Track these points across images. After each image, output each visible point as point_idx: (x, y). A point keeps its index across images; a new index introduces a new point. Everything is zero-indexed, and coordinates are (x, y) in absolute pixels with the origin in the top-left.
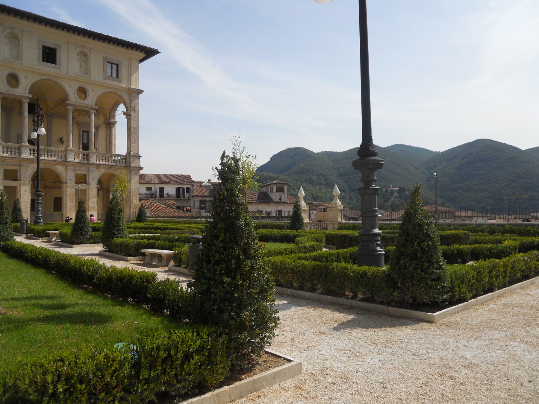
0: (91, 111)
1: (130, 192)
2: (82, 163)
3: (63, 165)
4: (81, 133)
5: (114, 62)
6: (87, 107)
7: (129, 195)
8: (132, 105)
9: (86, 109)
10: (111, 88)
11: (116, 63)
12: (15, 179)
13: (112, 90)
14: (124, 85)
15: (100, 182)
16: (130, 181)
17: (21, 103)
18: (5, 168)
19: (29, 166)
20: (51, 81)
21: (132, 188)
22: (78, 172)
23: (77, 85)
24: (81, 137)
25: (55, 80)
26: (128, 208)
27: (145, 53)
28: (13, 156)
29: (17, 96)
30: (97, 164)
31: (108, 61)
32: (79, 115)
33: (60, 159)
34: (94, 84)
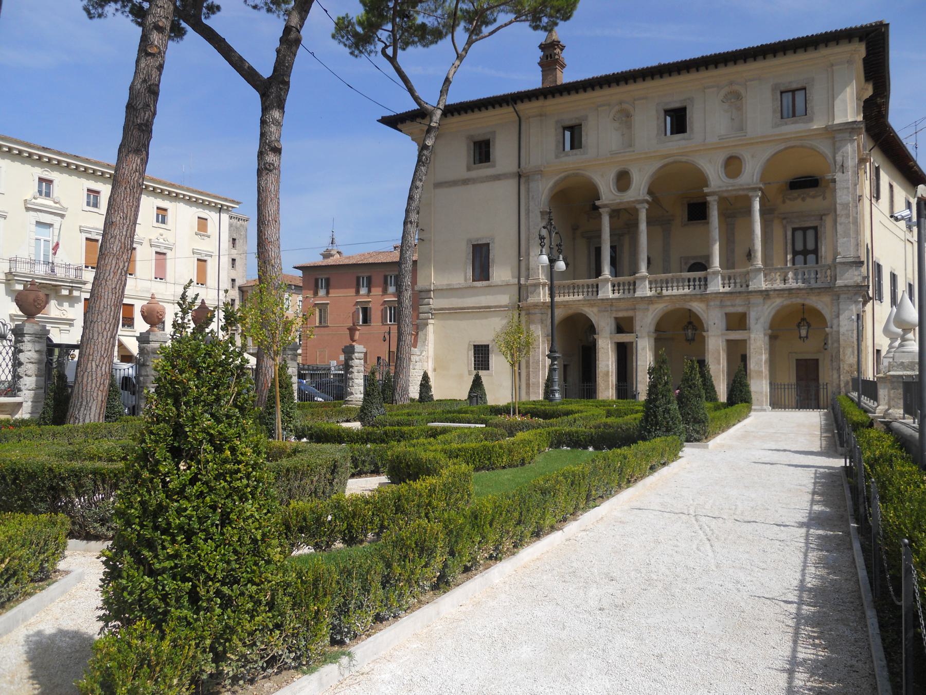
0: (751, 194)
4: (789, 234)
5: (794, 86)
6: (743, 190)
7: (836, 345)
8: (839, 158)
9: (741, 193)
10: (789, 139)
11: (799, 86)
12: (631, 331)
16: (838, 316)
18: (614, 315)
19: (647, 309)
21: (842, 330)
23: (721, 157)
25: (684, 159)
26: (835, 372)
27: (861, 40)
28: (627, 295)
29: (628, 202)
30: (761, 291)
31: (783, 89)
32: (784, 202)
33: (697, 291)
34: (752, 144)
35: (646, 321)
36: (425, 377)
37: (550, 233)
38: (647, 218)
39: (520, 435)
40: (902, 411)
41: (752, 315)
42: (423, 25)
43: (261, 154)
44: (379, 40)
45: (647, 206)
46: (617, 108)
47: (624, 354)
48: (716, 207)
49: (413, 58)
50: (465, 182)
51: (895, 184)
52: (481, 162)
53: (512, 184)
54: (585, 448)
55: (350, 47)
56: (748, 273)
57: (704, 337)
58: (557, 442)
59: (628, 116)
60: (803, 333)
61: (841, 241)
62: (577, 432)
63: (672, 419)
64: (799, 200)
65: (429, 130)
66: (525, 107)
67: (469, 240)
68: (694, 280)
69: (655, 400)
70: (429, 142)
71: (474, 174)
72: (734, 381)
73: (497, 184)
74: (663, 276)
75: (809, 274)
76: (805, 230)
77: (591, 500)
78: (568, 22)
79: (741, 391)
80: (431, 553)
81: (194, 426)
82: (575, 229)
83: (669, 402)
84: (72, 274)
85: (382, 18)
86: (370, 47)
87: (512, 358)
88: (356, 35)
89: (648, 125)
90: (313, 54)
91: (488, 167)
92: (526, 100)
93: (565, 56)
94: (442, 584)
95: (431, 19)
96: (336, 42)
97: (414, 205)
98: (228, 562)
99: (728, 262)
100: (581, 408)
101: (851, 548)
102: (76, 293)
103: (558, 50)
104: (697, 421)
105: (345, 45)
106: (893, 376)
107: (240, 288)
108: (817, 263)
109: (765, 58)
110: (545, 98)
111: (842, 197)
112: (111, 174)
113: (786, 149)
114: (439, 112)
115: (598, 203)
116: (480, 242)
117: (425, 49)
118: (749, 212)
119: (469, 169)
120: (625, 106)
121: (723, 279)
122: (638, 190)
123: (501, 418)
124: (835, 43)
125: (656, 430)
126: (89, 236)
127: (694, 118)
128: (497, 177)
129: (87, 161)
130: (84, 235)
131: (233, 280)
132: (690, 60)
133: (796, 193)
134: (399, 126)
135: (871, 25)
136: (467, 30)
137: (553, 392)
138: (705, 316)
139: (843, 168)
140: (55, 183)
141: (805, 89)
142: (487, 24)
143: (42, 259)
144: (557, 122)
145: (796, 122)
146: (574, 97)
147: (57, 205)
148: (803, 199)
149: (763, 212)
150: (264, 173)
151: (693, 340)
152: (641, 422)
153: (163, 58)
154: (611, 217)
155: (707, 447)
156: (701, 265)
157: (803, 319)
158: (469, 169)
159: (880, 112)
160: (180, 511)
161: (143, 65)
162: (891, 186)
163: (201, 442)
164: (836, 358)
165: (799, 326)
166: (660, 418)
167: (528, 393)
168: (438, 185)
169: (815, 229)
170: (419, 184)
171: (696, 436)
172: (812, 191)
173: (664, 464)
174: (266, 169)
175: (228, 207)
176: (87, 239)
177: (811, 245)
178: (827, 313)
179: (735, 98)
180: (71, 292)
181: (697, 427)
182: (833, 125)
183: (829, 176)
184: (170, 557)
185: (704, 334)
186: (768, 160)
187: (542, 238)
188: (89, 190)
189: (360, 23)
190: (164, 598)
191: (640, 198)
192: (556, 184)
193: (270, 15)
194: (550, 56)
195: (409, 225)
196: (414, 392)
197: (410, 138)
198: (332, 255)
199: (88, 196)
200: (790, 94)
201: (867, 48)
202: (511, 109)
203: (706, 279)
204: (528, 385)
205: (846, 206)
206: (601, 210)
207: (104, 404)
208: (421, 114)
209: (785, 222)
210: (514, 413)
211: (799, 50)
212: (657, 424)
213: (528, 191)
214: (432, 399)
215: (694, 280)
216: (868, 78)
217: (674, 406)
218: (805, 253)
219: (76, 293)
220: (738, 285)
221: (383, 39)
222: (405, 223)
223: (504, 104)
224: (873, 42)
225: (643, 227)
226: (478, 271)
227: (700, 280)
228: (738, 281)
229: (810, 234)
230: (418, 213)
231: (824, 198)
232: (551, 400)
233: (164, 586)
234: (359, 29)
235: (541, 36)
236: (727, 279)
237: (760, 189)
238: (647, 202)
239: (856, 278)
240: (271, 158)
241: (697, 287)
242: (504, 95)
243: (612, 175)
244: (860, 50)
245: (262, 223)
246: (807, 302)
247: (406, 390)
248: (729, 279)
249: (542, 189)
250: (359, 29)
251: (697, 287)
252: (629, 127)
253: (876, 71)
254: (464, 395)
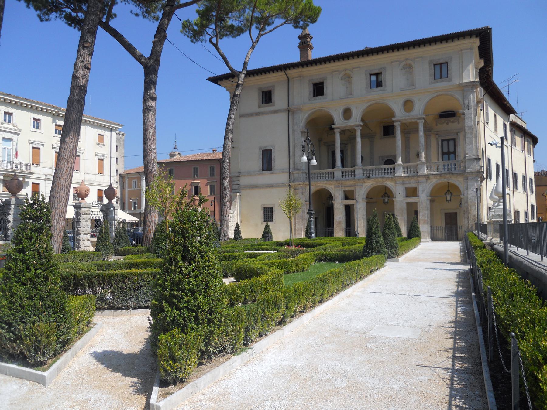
0: (418, 121)
1: (467, 202)
2: (408, 176)
5: (441, 61)
6: (414, 119)
7: (466, 205)
8: (466, 102)
9: (413, 121)
11: (444, 61)
13: (441, 93)
14: (456, 82)
15: (368, 197)
16: (467, 189)
17: (355, 131)
19: (362, 186)
20: (379, 103)
21: (470, 196)
22: (408, 186)
24: (440, 147)
25: (381, 101)
26: (466, 220)
27: (476, 37)
30: (425, 175)
31: (435, 63)
32: (437, 125)
35: (361, 192)
36: (237, 226)
37: (308, 143)
38: (361, 134)
39: (301, 256)
40: (499, 239)
41: (420, 189)
42: (232, 26)
43: (145, 101)
44: (207, 33)
45: (361, 128)
46: (343, 73)
47: (349, 210)
48: (399, 128)
49: (227, 44)
50: (258, 114)
51: (497, 115)
52: (266, 102)
53: (284, 115)
54: (334, 261)
55: (191, 38)
56: (417, 165)
57: (394, 201)
58: (320, 259)
59: (349, 77)
60: (449, 198)
61: (468, 147)
62: (329, 254)
63: (380, 246)
64: (445, 124)
65: (238, 86)
66: (290, 72)
67: (260, 148)
68: (388, 169)
69: (371, 236)
70: (238, 93)
71: (263, 109)
72: (411, 226)
73: (276, 115)
74: (371, 167)
75: (451, 165)
76: (448, 140)
77: (345, 286)
78: (314, 24)
79: (415, 231)
80: (279, 307)
81: (192, 247)
82: (320, 140)
83: (378, 237)
84: (24, 169)
85: (209, 21)
86: (201, 38)
87: (290, 216)
88: (194, 31)
89: (360, 82)
90: (173, 44)
91: (270, 106)
92: (292, 68)
93: (313, 42)
94: (282, 323)
95: (237, 22)
96: (183, 35)
97: (230, 128)
98: (210, 304)
99: (406, 160)
100: (328, 242)
101: (472, 304)
102: (27, 180)
103: (309, 39)
104: (392, 247)
105: (188, 36)
106: (494, 221)
107: (120, 175)
108: (455, 159)
109: (425, 46)
110: (303, 67)
111: (468, 123)
112: (63, 115)
113: (437, 96)
114: (243, 76)
115: (333, 126)
116: (266, 149)
117: (234, 39)
118: (417, 131)
119: (259, 107)
120: (348, 72)
121: (404, 168)
122: (355, 120)
123: (284, 248)
124: (463, 38)
125: (372, 252)
126: (34, 146)
127: (387, 78)
128: (276, 112)
129: (33, 102)
130: (32, 145)
131: (117, 170)
132: (384, 47)
133: (443, 120)
134: (219, 83)
135: (482, 29)
136: (257, 28)
137: (311, 233)
138: (394, 189)
139: (468, 107)
140: (14, 115)
141: (447, 63)
142: (269, 24)
143: (6, 160)
144: (309, 81)
145: (442, 81)
146: (319, 67)
147: (15, 128)
148: (447, 124)
149: (425, 131)
150: (147, 112)
151: (387, 203)
152: (364, 247)
153: (93, 49)
154: (341, 134)
155: (398, 261)
156: (391, 161)
157: (448, 191)
158: (259, 107)
159: (488, 75)
160: (189, 283)
161: (81, 53)
162: (495, 116)
163: (196, 254)
164: (467, 212)
165: (446, 194)
166: (374, 245)
167: (295, 234)
168: (242, 116)
169: (454, 140)
170: (232, 116)
171: (392, 255)
172: (452, 119)
173: (377, 269)
174: (148, 109)
175: (116, 128)
176: (33, 148)
177: (452, 150)
178: (461, 187)
179: (408, 68)
180: (24, 179)
181: (393, 250)
182: (462, 83)
183: (461, 111)
184: (186, 302)
185: (394, 199)
186: (428, 102)
187: (303, 147)
188: (34, 119)
189: (196, 24)
190: (184, 319)
191: (357, 123)
192: (309, 116)
193: (145, 19)
194: (304, 43)
195: (227, 140)
196: (231, 235)
197: (225, 89)
198: (175, 155)
199: (34, 122)
200: (439, 66)
201: (480, 41)
202: (283, 73)
203: (394, 169)
204: (295, 230)
205: (470, 128)
206: (335, 130)
207: (61, 244)
208: (232, 75)
209: (437, 136)
210: (291, 245)
211: (443, 42)
212: (372, 248)
213: (294, 120)
214: (242, 239)
215: (388, 169)
216: (481, 57)
217: (381, 239)
218: (449, 153)
219: (27, 180)
220: (412, 172)
221: (210, 33)
222: (225, 139)
223: (279, 70)
224: (484, 37)
225: (359, 139)
226: (265, 165)
227: (391, 169)
228: (412, 170)
229: (451, 143)
230: (232, 133)
231: (459, 123)
232: (310, 238)
233: (184, 315)
234: (196, 28)
235: (299, 32)
236: (406, 169)
237: (423, 118)
238: (361, 126)
239: (476, 168)
240: (150, 103)
241: (389, 173)
242: (279, 65)
243: (341, 111)
244: (476, 42)
245: (145, 140)
246: (450, 181)
247: (227, 233)
248: (407, 169)
249: (302, 119)
250: (196, 28)
251: (389, 173)
252: (350, 83)
253: (485, 52)
254: (260, 236)
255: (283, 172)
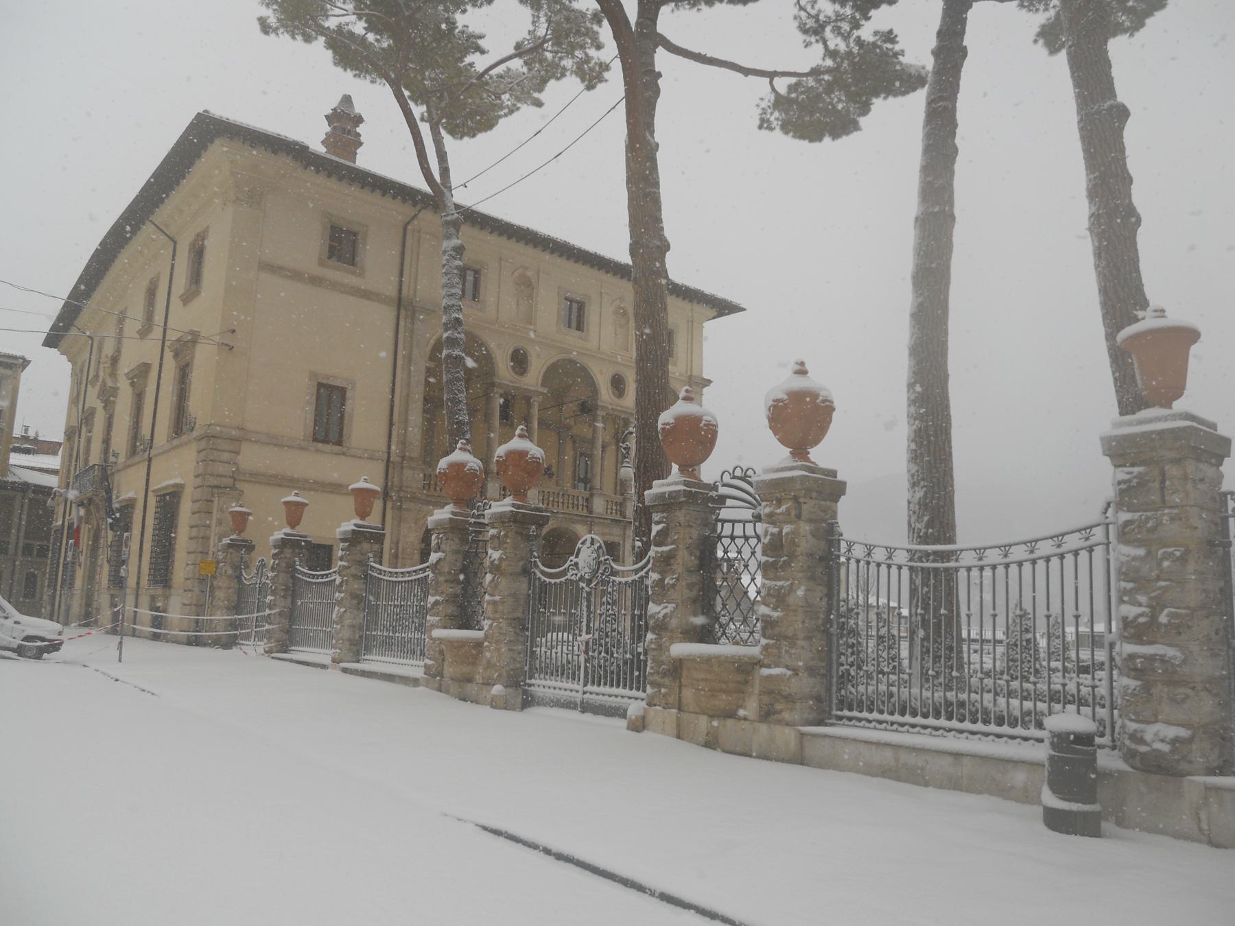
3: (585, 523)
22: (610, 539)
50: (316, 281)
53: (389, 313)
67: (313, 375)
128: (367, 295)
255: (371, 458)
